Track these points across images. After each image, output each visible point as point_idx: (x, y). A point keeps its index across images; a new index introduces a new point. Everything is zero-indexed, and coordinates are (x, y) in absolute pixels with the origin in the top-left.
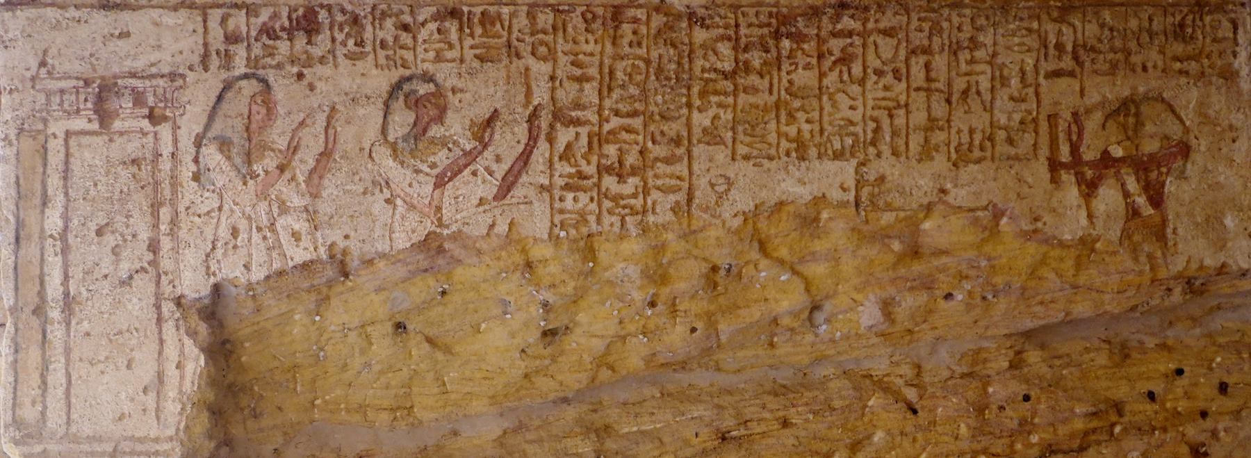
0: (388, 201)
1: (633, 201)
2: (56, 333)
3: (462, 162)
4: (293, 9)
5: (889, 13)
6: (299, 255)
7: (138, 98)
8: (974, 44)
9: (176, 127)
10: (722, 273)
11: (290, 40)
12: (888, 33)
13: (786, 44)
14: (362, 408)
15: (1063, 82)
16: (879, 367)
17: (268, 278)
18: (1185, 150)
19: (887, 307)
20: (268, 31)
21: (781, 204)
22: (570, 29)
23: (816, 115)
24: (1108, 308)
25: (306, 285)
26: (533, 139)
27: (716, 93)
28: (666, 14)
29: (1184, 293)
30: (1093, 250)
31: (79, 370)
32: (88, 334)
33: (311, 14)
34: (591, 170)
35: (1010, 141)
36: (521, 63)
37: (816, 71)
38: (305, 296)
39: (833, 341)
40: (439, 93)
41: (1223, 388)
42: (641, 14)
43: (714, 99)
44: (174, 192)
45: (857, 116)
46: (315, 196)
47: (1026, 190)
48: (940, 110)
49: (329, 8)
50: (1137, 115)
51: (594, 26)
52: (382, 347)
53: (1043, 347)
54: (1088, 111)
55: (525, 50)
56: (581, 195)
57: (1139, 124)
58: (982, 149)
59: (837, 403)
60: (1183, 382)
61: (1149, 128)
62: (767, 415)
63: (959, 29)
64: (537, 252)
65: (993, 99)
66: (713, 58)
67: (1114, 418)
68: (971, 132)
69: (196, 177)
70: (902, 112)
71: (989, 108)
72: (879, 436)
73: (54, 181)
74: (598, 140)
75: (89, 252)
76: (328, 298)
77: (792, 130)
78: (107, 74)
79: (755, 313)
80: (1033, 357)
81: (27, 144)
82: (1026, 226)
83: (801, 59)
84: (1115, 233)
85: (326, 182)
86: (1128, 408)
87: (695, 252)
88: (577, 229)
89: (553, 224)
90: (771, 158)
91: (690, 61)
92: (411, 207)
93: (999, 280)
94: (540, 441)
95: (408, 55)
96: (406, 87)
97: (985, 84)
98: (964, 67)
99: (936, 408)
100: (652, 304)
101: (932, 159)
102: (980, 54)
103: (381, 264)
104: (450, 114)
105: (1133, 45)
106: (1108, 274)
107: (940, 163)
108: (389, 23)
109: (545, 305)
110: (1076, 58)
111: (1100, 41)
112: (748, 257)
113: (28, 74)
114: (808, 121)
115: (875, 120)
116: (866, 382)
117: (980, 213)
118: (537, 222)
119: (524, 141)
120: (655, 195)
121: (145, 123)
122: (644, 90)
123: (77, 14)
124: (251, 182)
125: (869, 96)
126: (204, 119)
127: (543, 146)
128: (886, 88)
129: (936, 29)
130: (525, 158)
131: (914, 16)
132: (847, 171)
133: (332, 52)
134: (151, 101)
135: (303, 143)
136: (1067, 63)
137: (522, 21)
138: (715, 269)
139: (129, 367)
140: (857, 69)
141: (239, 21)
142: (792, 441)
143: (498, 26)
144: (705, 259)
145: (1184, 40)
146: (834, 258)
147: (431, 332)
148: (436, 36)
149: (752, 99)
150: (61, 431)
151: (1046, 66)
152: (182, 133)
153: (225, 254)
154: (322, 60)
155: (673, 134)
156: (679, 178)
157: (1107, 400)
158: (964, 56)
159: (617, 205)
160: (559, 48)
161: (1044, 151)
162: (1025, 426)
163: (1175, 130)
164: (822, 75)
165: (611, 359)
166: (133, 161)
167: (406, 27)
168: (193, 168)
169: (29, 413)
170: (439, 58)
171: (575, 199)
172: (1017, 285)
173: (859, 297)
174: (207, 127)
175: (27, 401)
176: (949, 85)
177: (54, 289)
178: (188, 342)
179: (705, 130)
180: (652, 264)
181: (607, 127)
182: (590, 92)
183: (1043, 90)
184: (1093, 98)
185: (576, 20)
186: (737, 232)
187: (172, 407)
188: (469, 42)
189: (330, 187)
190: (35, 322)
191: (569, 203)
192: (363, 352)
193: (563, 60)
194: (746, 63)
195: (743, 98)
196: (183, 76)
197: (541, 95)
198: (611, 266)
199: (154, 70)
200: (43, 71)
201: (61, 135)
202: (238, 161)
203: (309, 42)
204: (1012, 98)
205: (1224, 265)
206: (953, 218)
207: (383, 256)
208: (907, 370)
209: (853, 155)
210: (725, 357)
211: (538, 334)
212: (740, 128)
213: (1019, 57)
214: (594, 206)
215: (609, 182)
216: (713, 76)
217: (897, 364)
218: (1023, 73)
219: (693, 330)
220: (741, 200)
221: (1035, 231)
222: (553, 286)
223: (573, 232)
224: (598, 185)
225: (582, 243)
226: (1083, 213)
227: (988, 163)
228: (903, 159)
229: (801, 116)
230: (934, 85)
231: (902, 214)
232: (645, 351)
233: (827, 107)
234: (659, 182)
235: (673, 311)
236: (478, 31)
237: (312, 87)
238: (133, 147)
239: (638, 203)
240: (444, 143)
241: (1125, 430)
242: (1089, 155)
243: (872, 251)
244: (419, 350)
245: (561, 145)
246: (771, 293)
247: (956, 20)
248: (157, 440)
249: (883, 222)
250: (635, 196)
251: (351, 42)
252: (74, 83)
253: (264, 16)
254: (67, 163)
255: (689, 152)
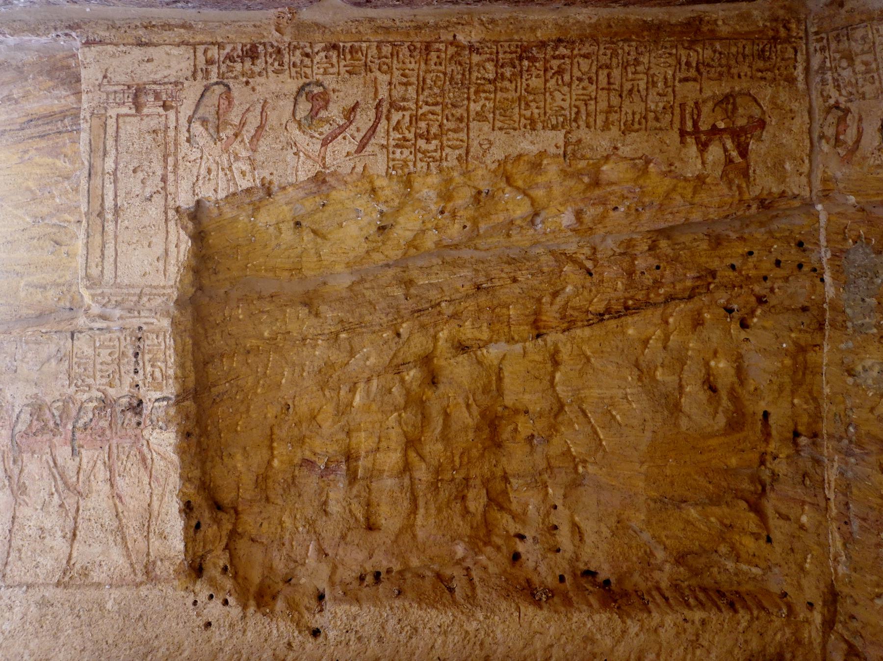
0: (295, 154)
1: (434, 154)
2: (110, 227)
3: (338, 131)
4: (244, 45)
5: (587, 45)
6: (244, 184)
7: (157, 96)
8: (637, 62)
9: (177, 112)
10: (484, 194)
11: (242, 62)
12: (586, 56)
13: (526, 63)
14: (273, 269)
15: (690, 84)
16: (571, 248)
17: (227, 197)
18: (762, 124)
19: (579, 214)
20: (230, 58)
21: (520, 156)
22: (401, 56)
23: (542, 104)
24: (711, 216)
25: (248, 200)
26: (378, 119)
27: (485, 92)
28: (457, 46)
29: (758, 208)
30: (704, 183)
31: (122, 248)
32: (127, 228)
33: (254, 47)
34: (410, 136)
35: (657, 119)
36: (372, 75)
37: (543, 79)
38: (247, 207)
39: (545, 234)
40: (325, 92)
41: (778, 263)
42: (442, 46)
43: (483, 95)
44: (176, 148)
45: (566, 105)
46: (254, 151)
47: (665, 147)
48: (615, 101)
49: (264, 44)
50: (734, 104)
51: (415, 54)
52: (288, 235)
53: (669, 238)
54: (704, 102)
55: (375, 67)
56: (405, 150)
57: (735, 108)
58: (640, 123)
59: (545, 269)
60: (752, 260)
61: (741, 111)
62: (504, 275)
63: (629, 54)
64: (378, 183)
65: (647, 94)
66: (482, 71)
67: (710, 280)
68: (634, 114)
69: (188, 140)
70: (593, 102)
71: (644, 100)
72: (569, 289)
73: (110, 143)
74: (415, 119)
75: (131, 183)
76: (259, 208)
77: (528, 113)
78: (140, 82)
79: (501, 217)
80: (663, 244)
81: (96, 122)
82: (664, 168)
83: (534, 72)
84: (718, 172)
85: (260, 143)
86: (718, 274)
87: (469, 183)
88: (402, 169)
89: (388, 167)
90: (515, 129)
91: (470, 73)
92: (308, 157)
93: (646, 200)
94: (373, 288)
95: (308, 71)
96: (307, 89)
97: (642, 85)
98: (630, 76)
99: (603, 273)
100: (442, 212)
101: (609, 129)
102: (640, 68)
103: (290, 189)
104: (331, 104)
105: (733, 62)
106: (712, 197)
107: (614, 131)
108: (298, 53)
109: (381, 212)
110: (698, 70)
111: (713, 60)
112: (499, 186)
113: (97, 83)
114: (537, 108)
115: (576, 106)
116: (563, 258)
117: (637, 161)
118: (379, 165)
119: (373, 120)
120: (447, 150)
121: (161, 110)
122: (443, 90)
123: (124, 49)
124: (219, 143)
125: (574, 93)
126: (193, 107)
127: (384, 122)
128: (584, 89)
129: (615, 54)
130: (373, 129)
131: (602, 47)
132: (560, 135)
133: (265, 69)
134: (164, 97)
135: (248, 121)
136: (693, 73)
137: (373, 51)
138: (479, 192)
139: (149, 246)
140: (567, 78)
141: (214, 52)
142: (518, 290)
143: (360, 54)
144: (474, 187)
145: (764, 60)
146: (549, 187)
147: (314, 227)
148: (324, 60)
149: (505, 95)
150: (112, 282)
151: (679, 75)
152: (181, 115)
153: (203, 184)
154: (260, 74)
155: (458, 115)
156: (461, 141)
157: (707, 269)
158: (630, 69)
159: (426, 156)
160: (394, 67)
161: (677, 125)
162: (657, 284)
163: (756, 112)
164: (546, 81)
165: (416, 243)
166: (154, 131)
167: (307, 55)
168: (187, 135)
169: (94, 272)
170: (325, 73)
171: (401, 153)
172: (657, 203)
173: (562, 209)
174: (195, 112)
175: (93, 265)
176: (622, 86)
177: (109, 203)
178: (182, 232)
179: (477, 113)
180: (444, 190)
181: (420, 112)
182: (411, 91)
183: (676, 89)
184: (708, 93)
185: (404, 51)
186: (494, 172)
187: (173, 269)
188: (343, 63)
189: (263, 145)
190: (99, 221)
191: (398, 155)
192: (276, 238)
193: (397, 73)
194: (502, 74)
195: (499, 95)
196: (182, 84)
197: (383, 93)
198: (420, 191)
199: (166, 80)
200: (105, 80)
201: (114, 117)
202: (212, 131)
203: (253, 64)
204: (658, 94)
205: (784, 192)
206: (621, 164)
207: (291, 185)
208: (587, 251)
209: (563, 127)
210: (480, 243)
211: (375, 229)
212: (497, 112)
213: (662, 70)
214: (412, 157)
215: (421, 143)
216: (482, 82)
217: (582, 247)
218: (665, 78)
219: (465, 227)
220: (497, 153)
221: (670, 171)
222: (386, 202)
223: (400, 171)
224: (415, 145)
225: (405, 178)
226: (699, 161)
227: (643, 132)
228: (592, 129)
229: (533, 105)
230: (612, 87)
231: (591, 162)
232: (436, 239)
233: (549, 100)
234: (450, 143)
235: (454, 216)
236: (348, 57)
237: (254, 89)
238: (153, 123)
239: (437, 155)
240: (327, 121)
241: (717, 287)
242: (704, 127)
243: (570, 183)
244: (308, 237)
245: (394, 122)
246: (510, 206)
247: (626, 49)
248: (164, 287)
249: (579, 166)
250: (436, 151)
251: (276, 64)
252: (122, 87)
253: (228, 49)
254: (117, 132)
255: (468, 125)
